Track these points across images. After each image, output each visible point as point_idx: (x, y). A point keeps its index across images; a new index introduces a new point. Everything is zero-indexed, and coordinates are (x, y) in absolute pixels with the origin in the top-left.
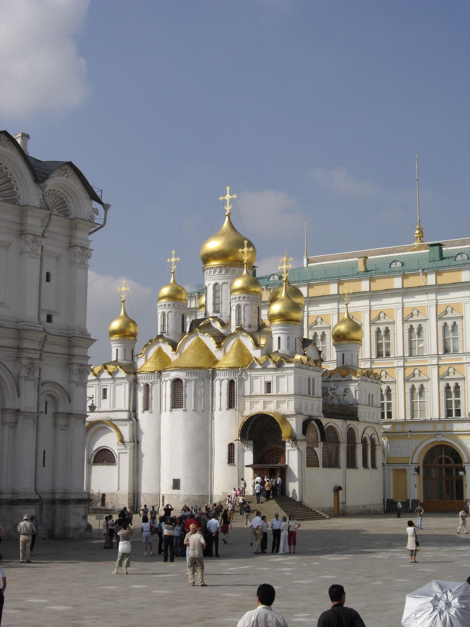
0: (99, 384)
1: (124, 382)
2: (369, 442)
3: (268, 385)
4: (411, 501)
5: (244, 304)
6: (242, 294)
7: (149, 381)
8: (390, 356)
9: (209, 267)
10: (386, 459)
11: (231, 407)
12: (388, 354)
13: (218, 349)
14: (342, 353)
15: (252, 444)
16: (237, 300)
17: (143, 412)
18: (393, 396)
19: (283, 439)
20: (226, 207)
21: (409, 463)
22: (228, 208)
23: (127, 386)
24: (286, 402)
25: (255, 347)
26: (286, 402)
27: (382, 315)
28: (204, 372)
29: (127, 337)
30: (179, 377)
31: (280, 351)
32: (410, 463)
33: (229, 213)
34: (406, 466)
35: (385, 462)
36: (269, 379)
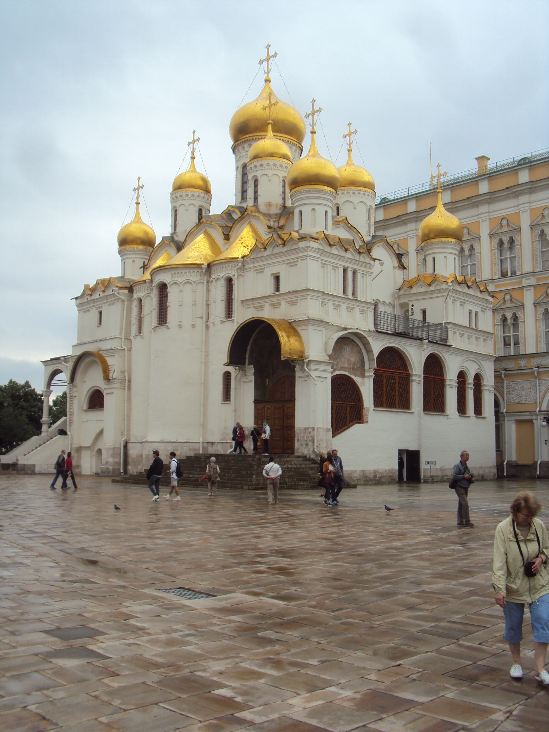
1: (115, 300)
2: (470, 380)
3: (277, 278)
4: (539, 463)
8: (516, 273)
10: (506, 407)
11: (229, 317)
12: (513, 273)
13: (226, 241)
14: (432, 256)
15: (253, 371)
18: (521, 326)
19: (282, 357)
21: (536, 411)
24: (299, 301)
27: (504, 222)
28: (196, 271)
31: (300, 232)
32: (538, 410)
34: (532, 415)
35: (505, 411)
36: (275, 270)
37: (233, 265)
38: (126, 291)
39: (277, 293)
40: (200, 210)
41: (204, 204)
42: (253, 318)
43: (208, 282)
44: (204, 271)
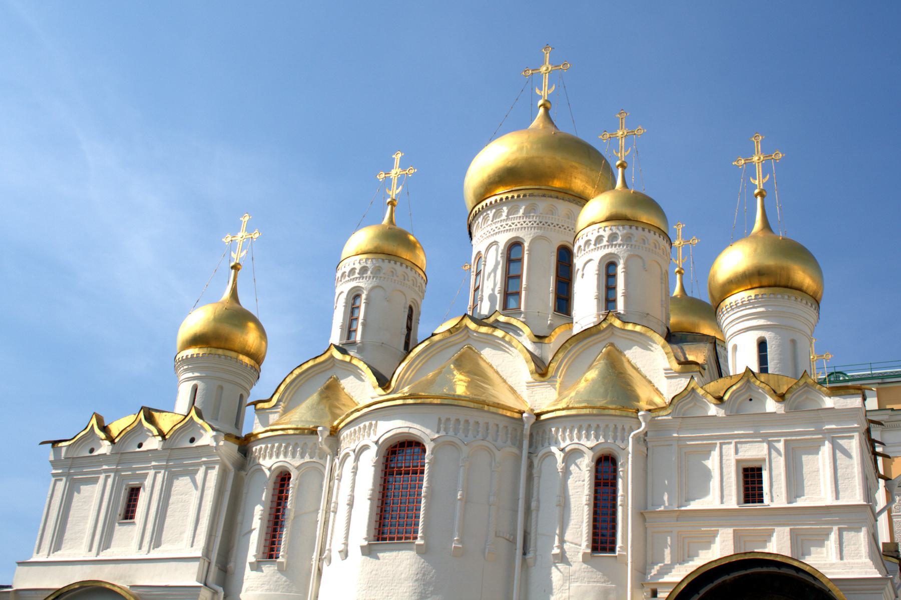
0: (116, 472)
5: (626, 255)
6: (621, 228)
7: (293, 462)
9: (498, 198)
11: (604, 550)
13: (537, 376)
16: (605, 243)
17: (256, 567)
20: (541, 90)
22: (544, 92)
23: (213, 475)
25: (676, 366)
26: (833, 536)
29: (233, 354)
30: (412, 431)
33: (547, 101)
37: (620, 428)
38: (232, 448)
39: (757, 506)
40: (411, 309)
41: (418, 299)
42: (745, 553)
43: (529, 458)
44: (527, 427)
